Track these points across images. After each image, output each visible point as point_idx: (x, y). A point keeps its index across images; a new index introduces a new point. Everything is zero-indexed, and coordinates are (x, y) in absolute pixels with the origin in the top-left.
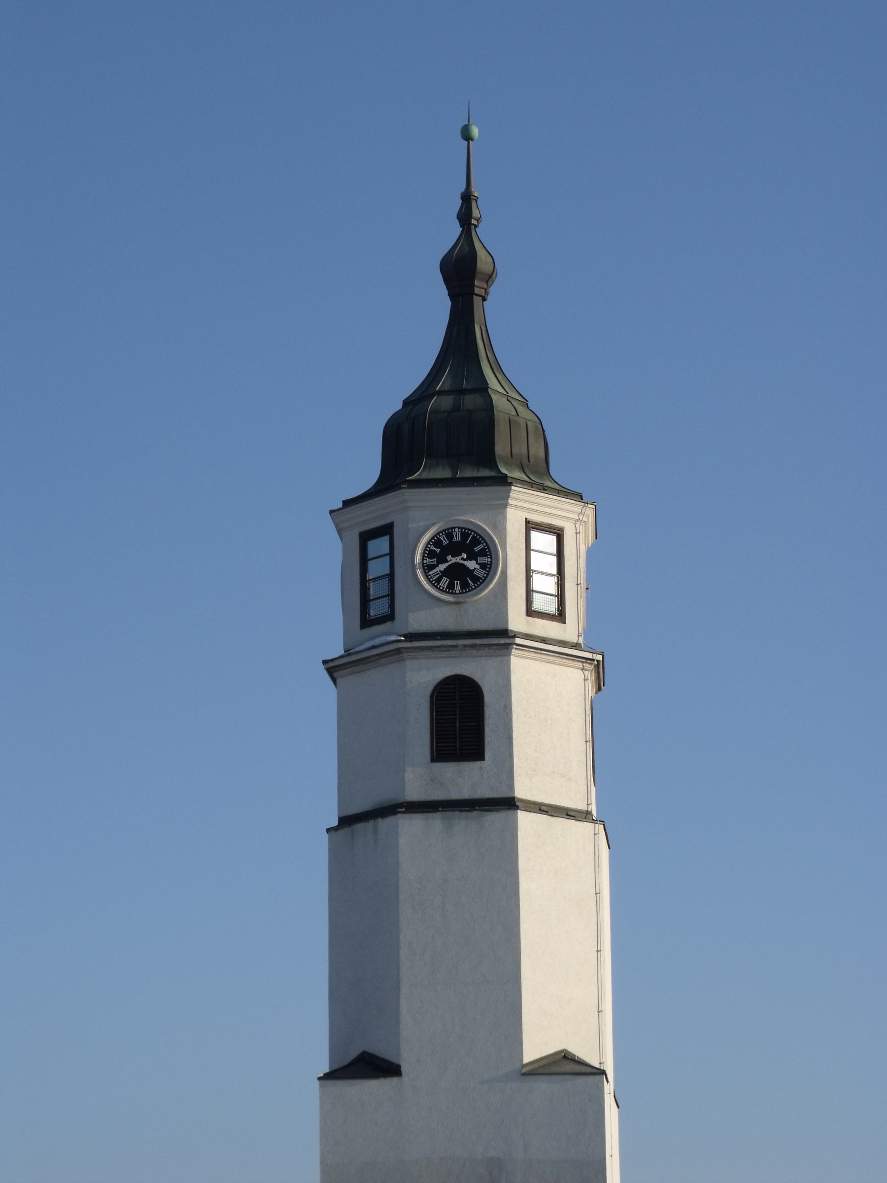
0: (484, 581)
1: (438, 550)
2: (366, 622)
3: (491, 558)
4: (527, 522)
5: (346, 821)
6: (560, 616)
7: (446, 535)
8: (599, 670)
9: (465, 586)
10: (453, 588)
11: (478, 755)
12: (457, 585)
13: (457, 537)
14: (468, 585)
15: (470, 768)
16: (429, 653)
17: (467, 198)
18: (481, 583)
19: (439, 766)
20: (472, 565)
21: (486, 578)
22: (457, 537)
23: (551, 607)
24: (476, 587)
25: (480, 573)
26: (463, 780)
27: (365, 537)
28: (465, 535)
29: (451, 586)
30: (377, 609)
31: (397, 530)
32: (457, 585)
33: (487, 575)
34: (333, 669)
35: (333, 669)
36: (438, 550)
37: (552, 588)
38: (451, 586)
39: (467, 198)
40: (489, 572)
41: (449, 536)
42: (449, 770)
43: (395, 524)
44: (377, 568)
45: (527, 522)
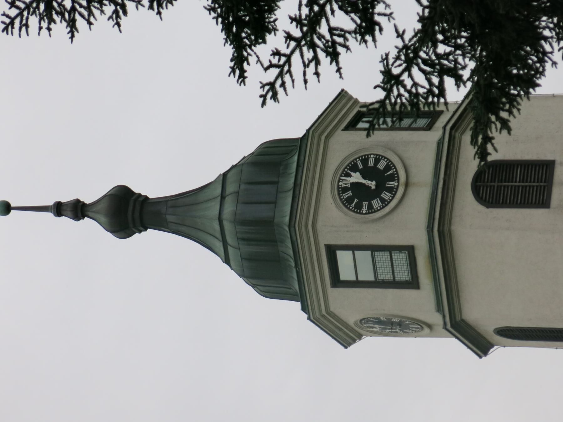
0: (390, 161)
1: (356, 201)
3: (371, 155)
7: (343, 193)
9: (394, 177)
10: (393, 188)
14: (392, 175)
16: (448, 205)
17: (59, 209)
18: (392, 163)
21: (388, 159)
24: (395, 168)
31: (333, 242)
33: (385, 158)
36: (356, 201)
39: (59, 209)
40: (383, 157)
43: (327, 243)
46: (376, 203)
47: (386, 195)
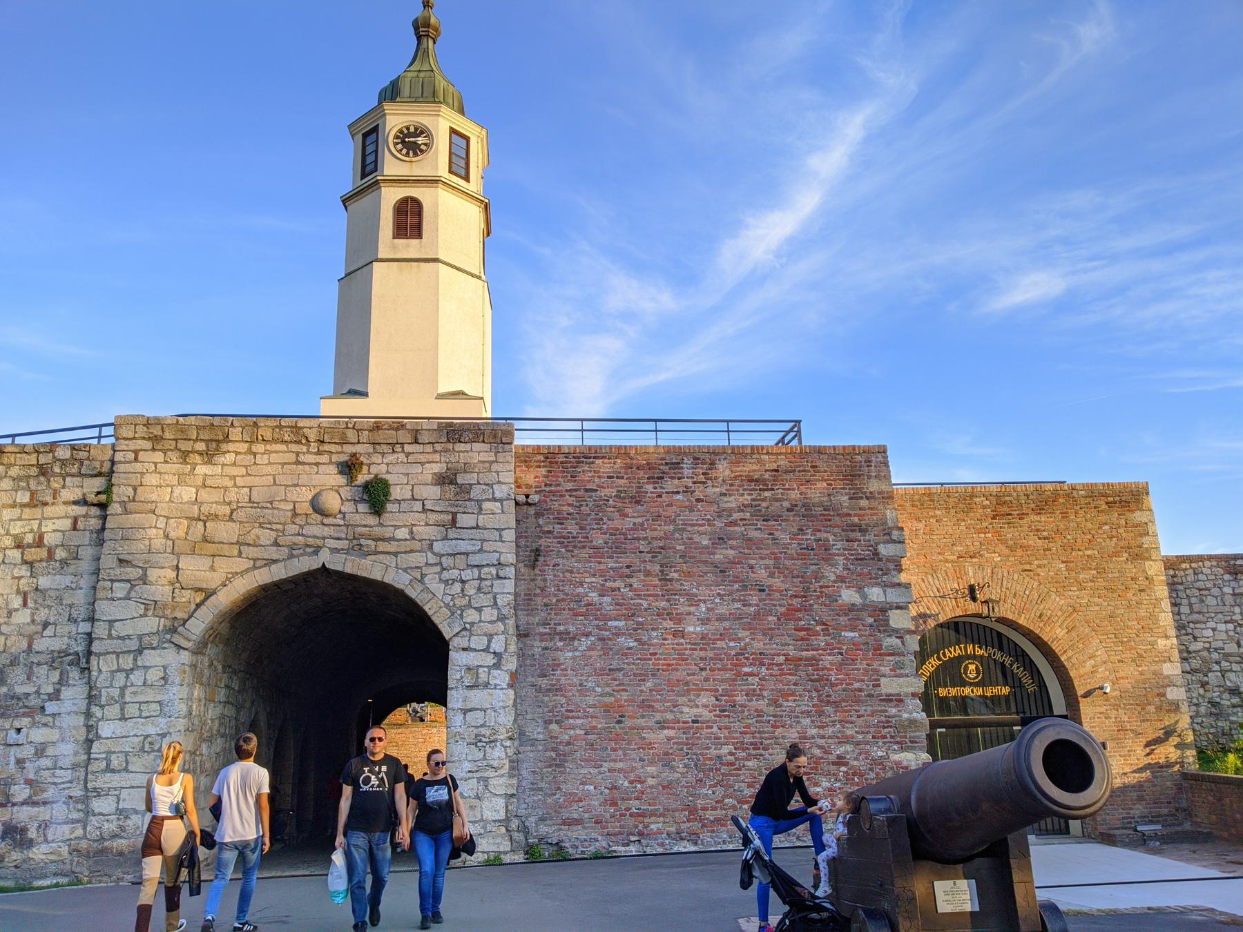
2: (363, 176)
4: (451, 128)
5: (347, 275)
6: (467, 179)
8: (487, 208)
9: (415, 155)
11: (419, 235)
12: (411, 153)
13: (412, 130)
15: (415, 242)
19: (396, 241)
20: (420, 140)
22: (412, 130)
23: (463, 173)
25: (423, 147)
26: (410, 248)
27: (365, 136)
28: (416, 129)
29: (408, 154)
30: (368, 169)
32: (411, 153)
34: (346, 201)
35: (346, 201)
37: (463, 164)
38: (408, 154)
41: (408, 128)
42: (401, 242)
44: (370, 149)
45: (451, 128)
46: (400, 146)
47: (404, 151)
